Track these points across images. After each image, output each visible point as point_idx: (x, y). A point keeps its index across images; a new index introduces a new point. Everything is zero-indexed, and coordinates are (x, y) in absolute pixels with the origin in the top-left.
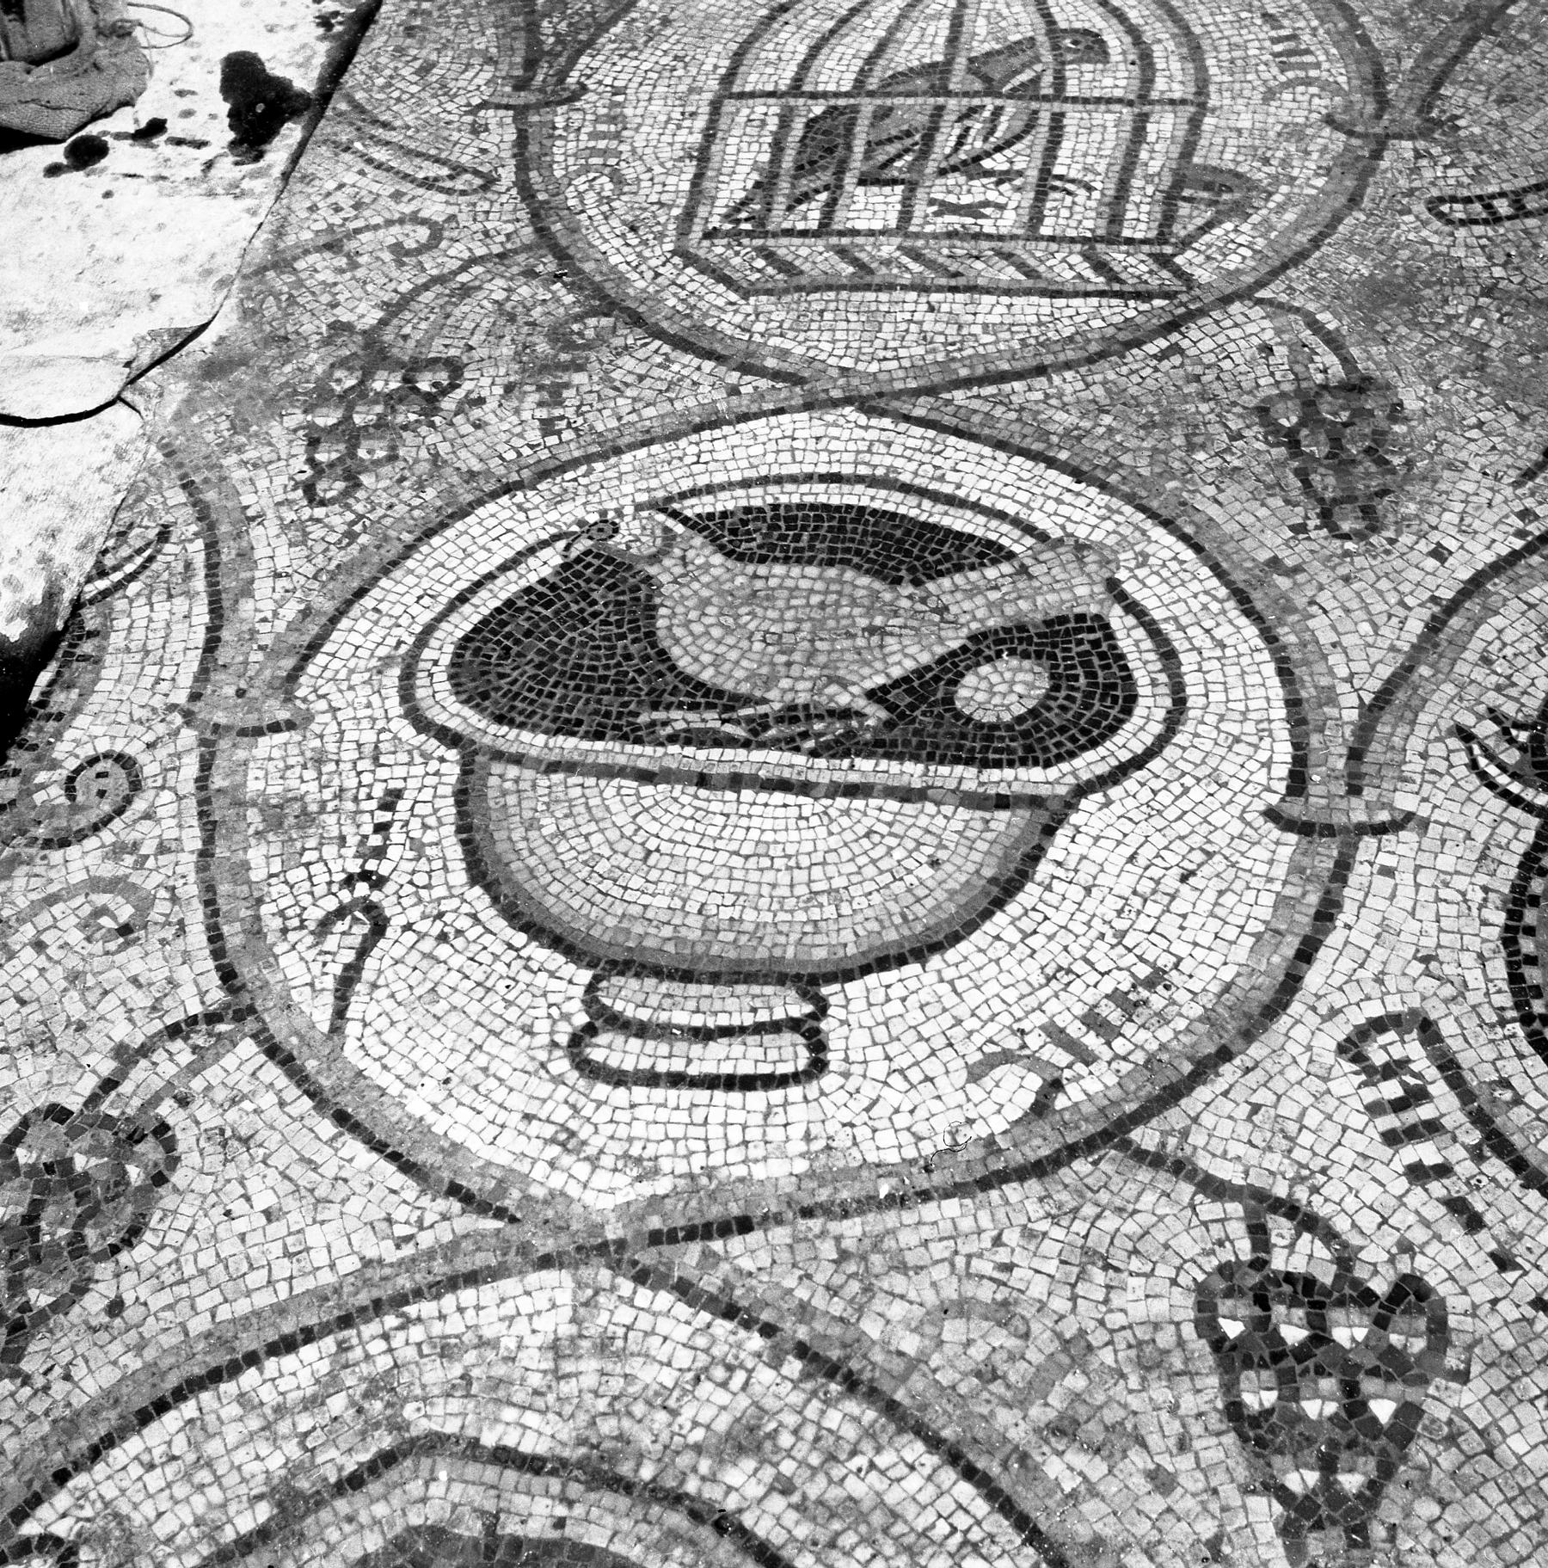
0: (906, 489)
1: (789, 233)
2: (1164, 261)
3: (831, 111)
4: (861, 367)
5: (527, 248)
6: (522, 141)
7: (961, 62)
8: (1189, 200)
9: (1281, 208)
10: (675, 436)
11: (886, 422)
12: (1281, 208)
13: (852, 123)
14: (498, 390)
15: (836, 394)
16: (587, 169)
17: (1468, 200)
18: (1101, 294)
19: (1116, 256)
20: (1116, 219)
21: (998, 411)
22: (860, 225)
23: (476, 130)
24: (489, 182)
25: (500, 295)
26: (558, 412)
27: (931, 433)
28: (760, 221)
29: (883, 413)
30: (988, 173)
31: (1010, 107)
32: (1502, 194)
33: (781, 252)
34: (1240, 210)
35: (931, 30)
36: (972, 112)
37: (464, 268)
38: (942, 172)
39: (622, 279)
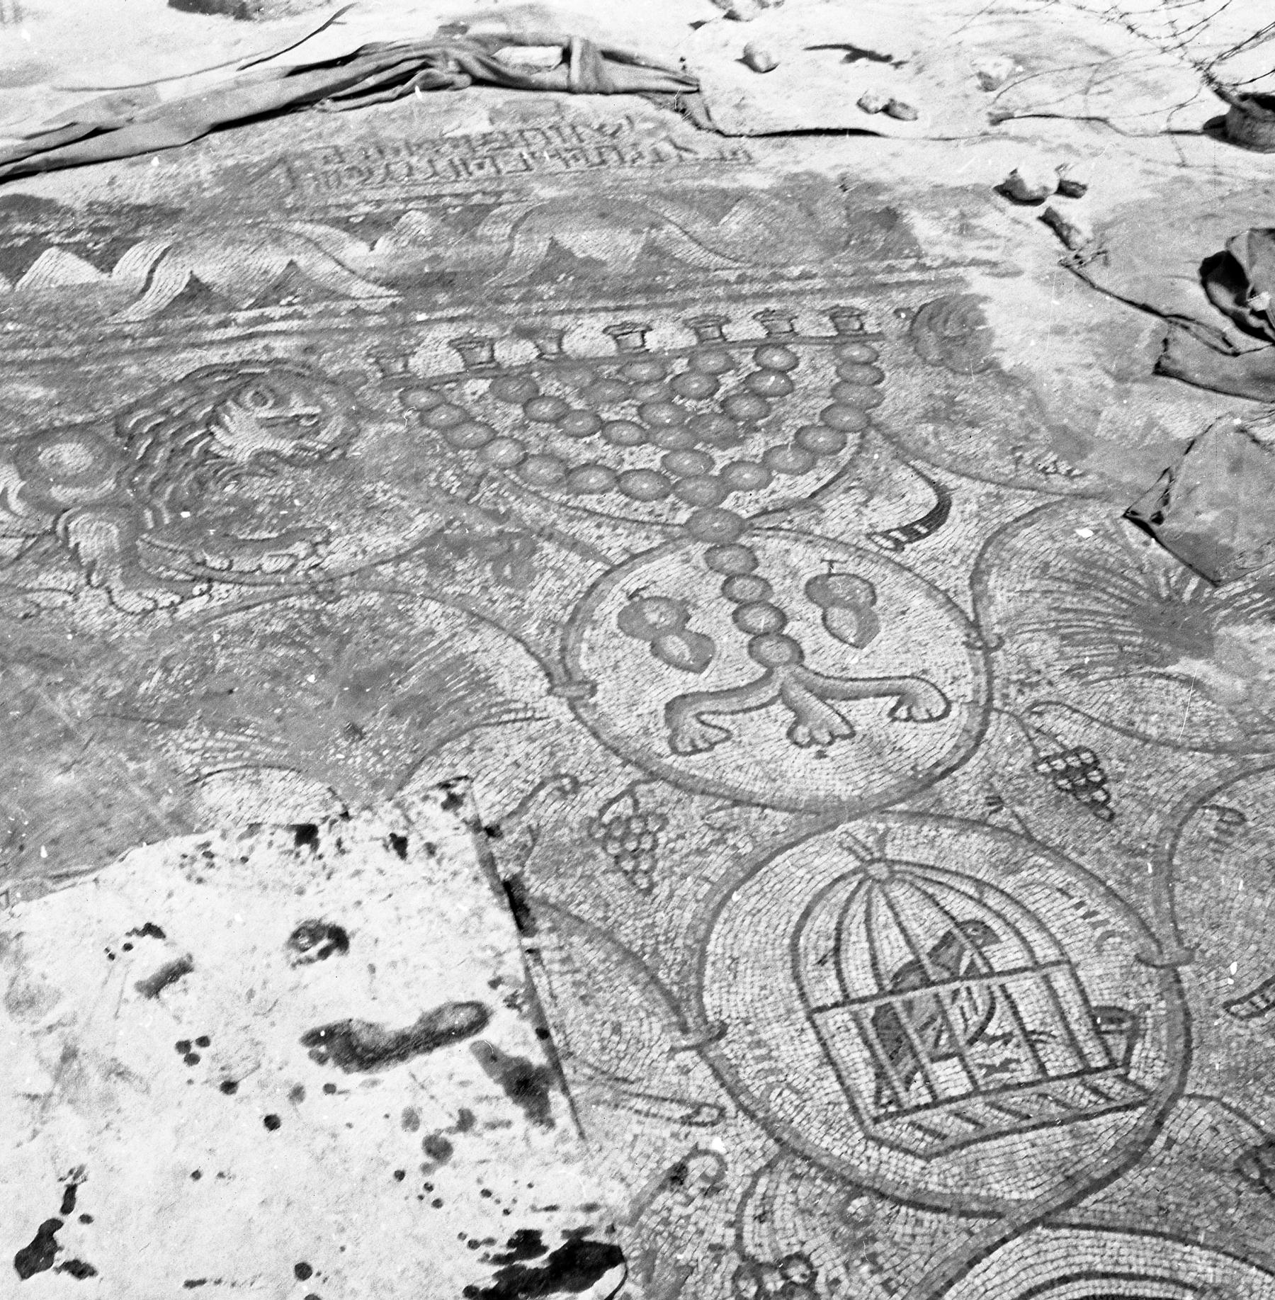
0: (1105, 1275)
1: (918, 1108)
2: (1124, 1078)
3: (878, 1009)
4: (1024, 1196)
5: (779, 1157)
6: (717, 1074)
7: (923, 957)
8: (1108, 1032)
9: (1156, 1028)
10: (961, 1275)
11: (1065, 1232)
12: (1156, 1028)
13: (896, 1017)
14: (842, 1270)
15: (1025, 1220)
16: (770, 1087)
17: (1239, 1002)
18: (1109, 1111)
19: (1098, 1080)
20: (1081, 1056)
21: (1114, 1207)
22: (954, 1092)
23: (685, 1071)
24: (722, 1111)
25: (791, 1198)
26: (886, 1276)
27: (1092, 1233)
28: (895, 1100)
29: (1058, 1226)
30: (994, 1039)
31: (972, 984)
32: (1253, 994)
33: (925, 1123)
34: (1134, 1035)
35: (892, 938)
36: (955, 993)
37: (754, 1184)
38: (971, 1042)
39: (852, 1168)
